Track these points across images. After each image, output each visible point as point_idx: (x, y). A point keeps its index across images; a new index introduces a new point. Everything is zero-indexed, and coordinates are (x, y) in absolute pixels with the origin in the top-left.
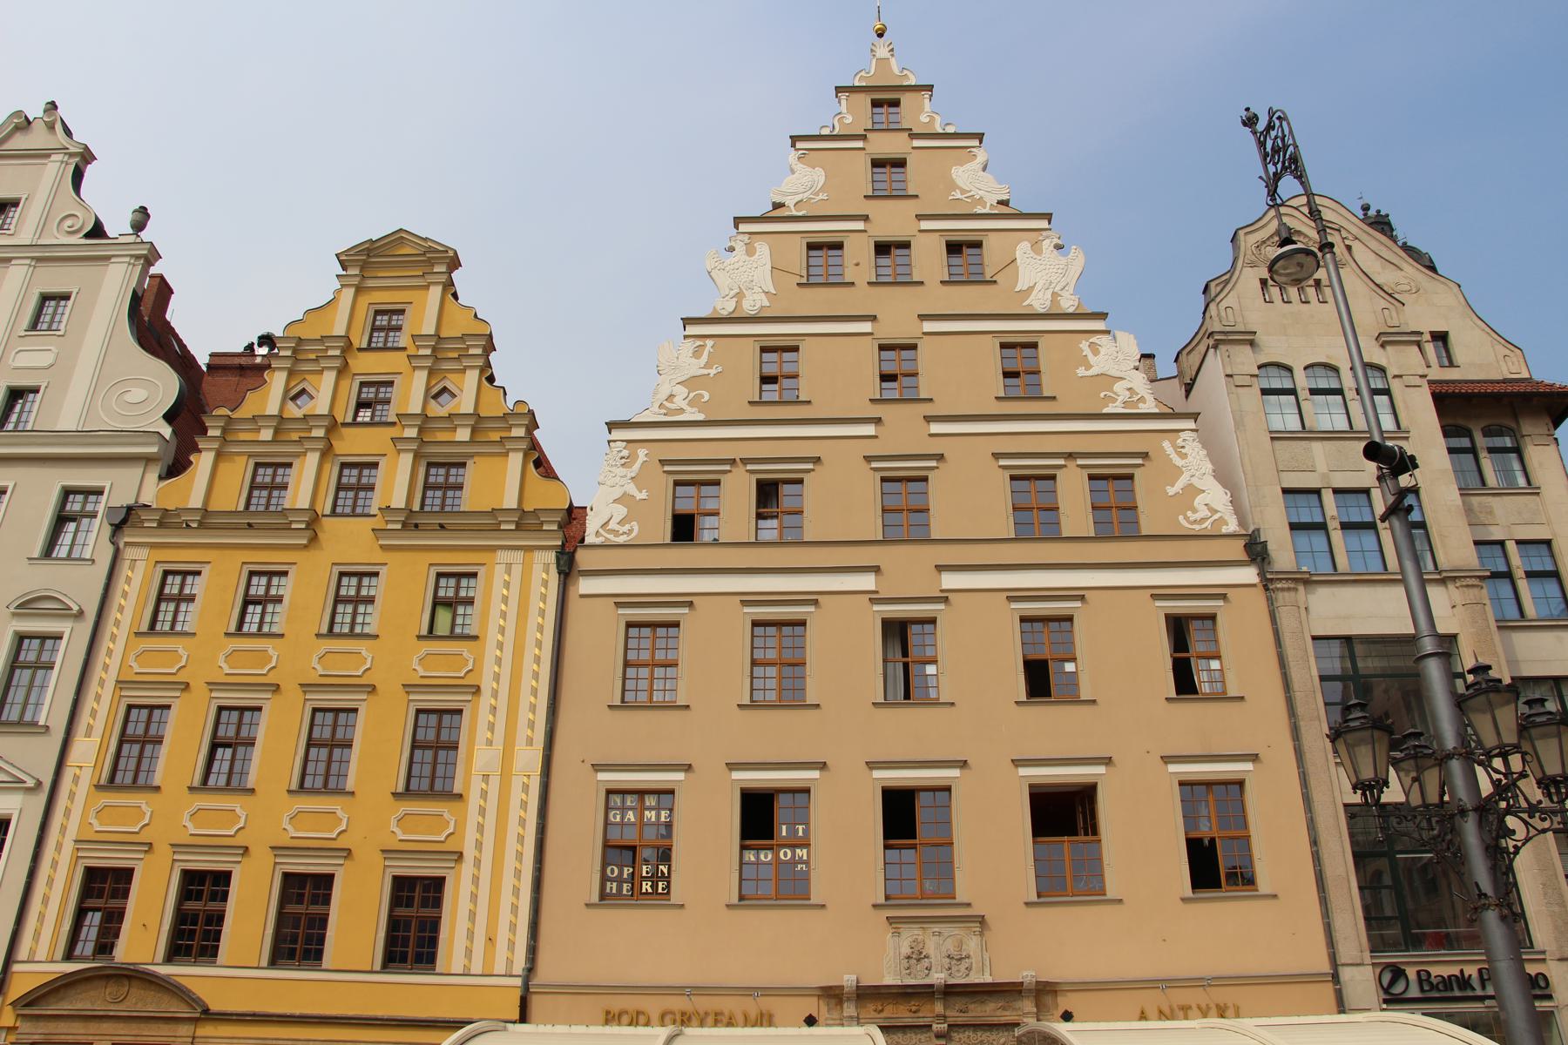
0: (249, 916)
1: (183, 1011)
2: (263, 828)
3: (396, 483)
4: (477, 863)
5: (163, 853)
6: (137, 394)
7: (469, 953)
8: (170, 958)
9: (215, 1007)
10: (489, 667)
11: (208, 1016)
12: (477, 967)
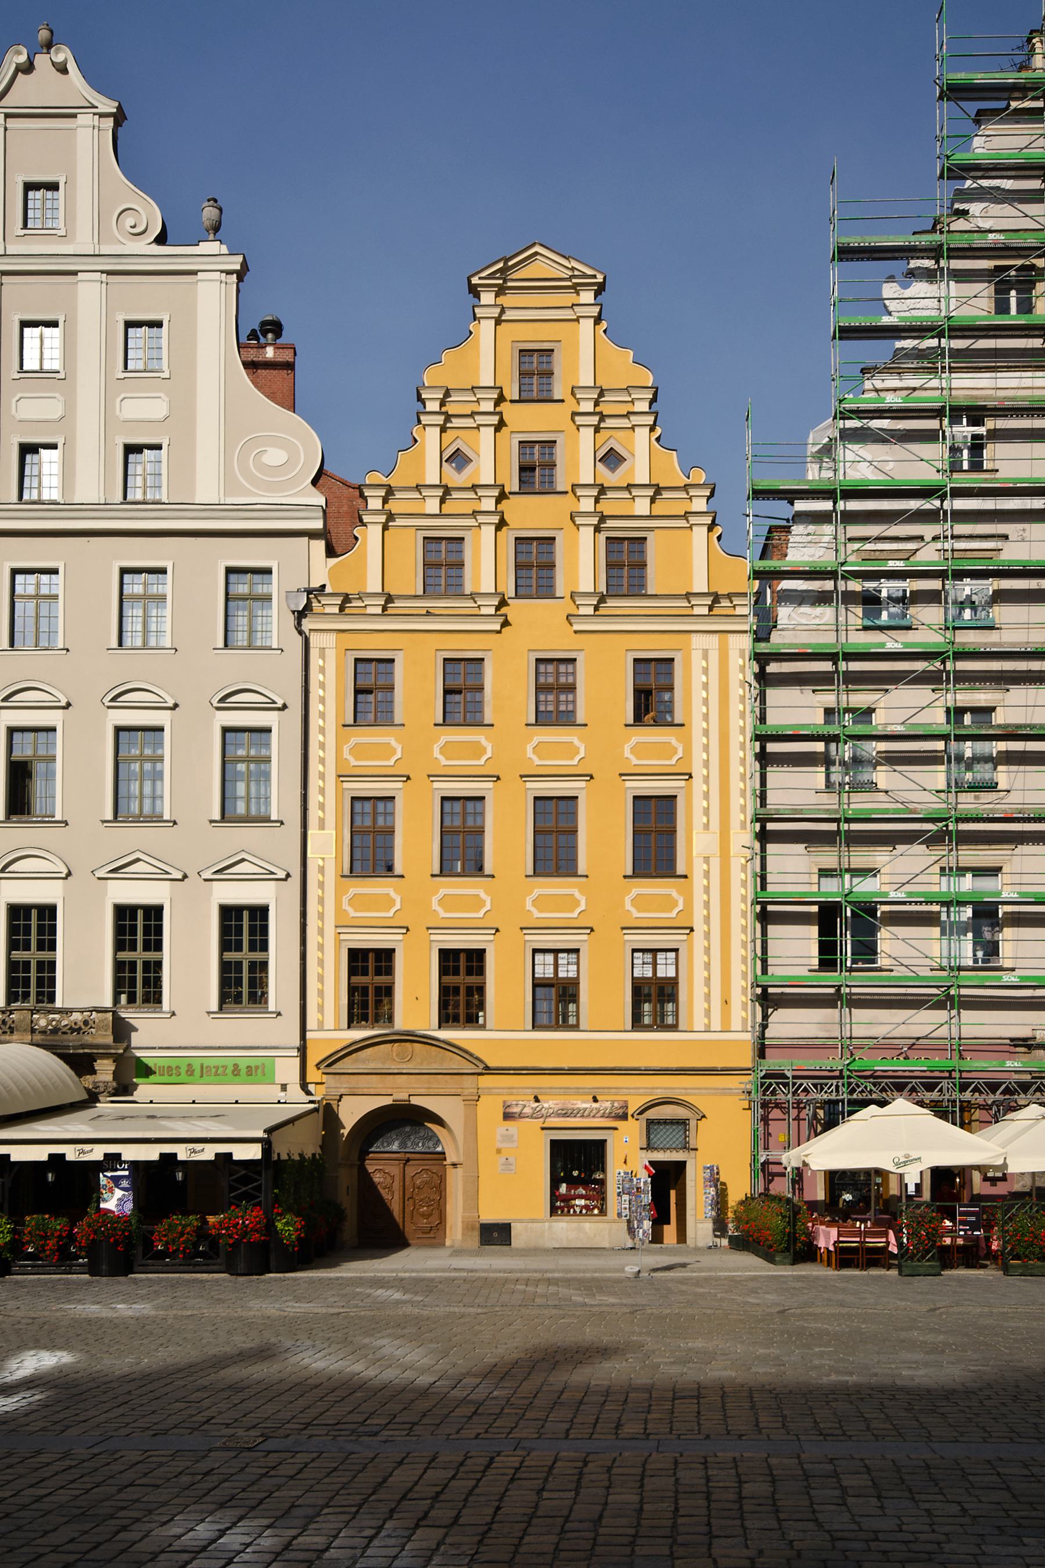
0: (506, 988)
1: (469, 1068)
2: (506, 911)
3: (581, 563)
4: (707, 935)
6: (275, 456)
7: (708, 1013)
10: (699, 756)
11: (488, 1070)
12: (716, 1025)
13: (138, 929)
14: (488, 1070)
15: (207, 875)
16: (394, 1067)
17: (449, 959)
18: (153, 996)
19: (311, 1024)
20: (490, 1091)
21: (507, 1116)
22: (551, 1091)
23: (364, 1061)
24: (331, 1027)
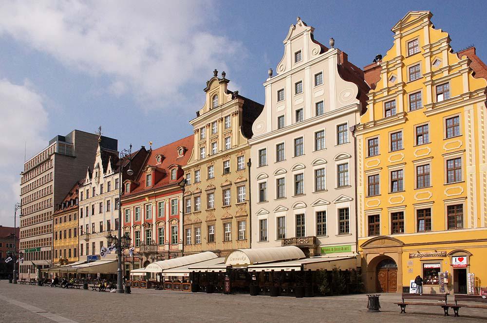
1: (399, 244)
5: (385, 209)
8: (392, 234)
9: (405, 243)
11: (404, 245)
13: (321, 216)
14: (404, 245)
15: (334, 202)
16: (379, 246)
17: (394, 216)
18: (325, 233)
19: (359, 236)
20: (405, 251)
21: (410, 257)
22: (423, 250)
23: (373, 245)
24: (364, 236)
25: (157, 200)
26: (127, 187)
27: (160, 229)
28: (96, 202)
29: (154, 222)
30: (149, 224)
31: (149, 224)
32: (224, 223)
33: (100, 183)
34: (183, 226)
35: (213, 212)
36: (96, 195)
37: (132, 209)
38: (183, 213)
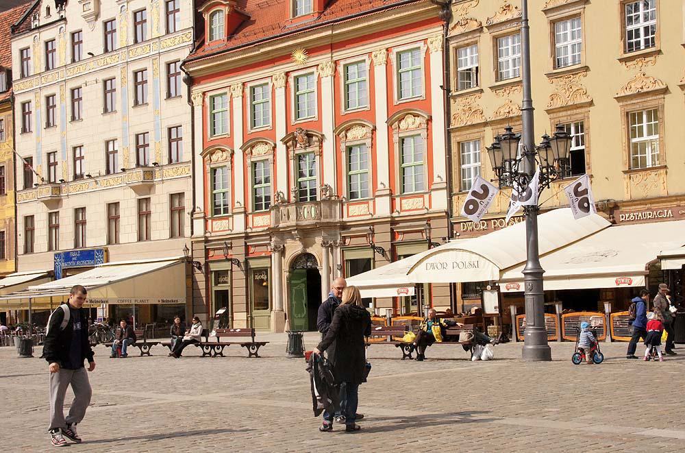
25: (338, 55)
26: (211, 23)
27: (254, 164)
28: (91, 79)
29: (328, 129)
30: (310, 136)
31: (310, 136)
32: (629, 109)
33: (104, 16)
34: (448, 133)
35: (582, 81)
36: (85, 56)
37: (238, 92)
38: (446, 89)
